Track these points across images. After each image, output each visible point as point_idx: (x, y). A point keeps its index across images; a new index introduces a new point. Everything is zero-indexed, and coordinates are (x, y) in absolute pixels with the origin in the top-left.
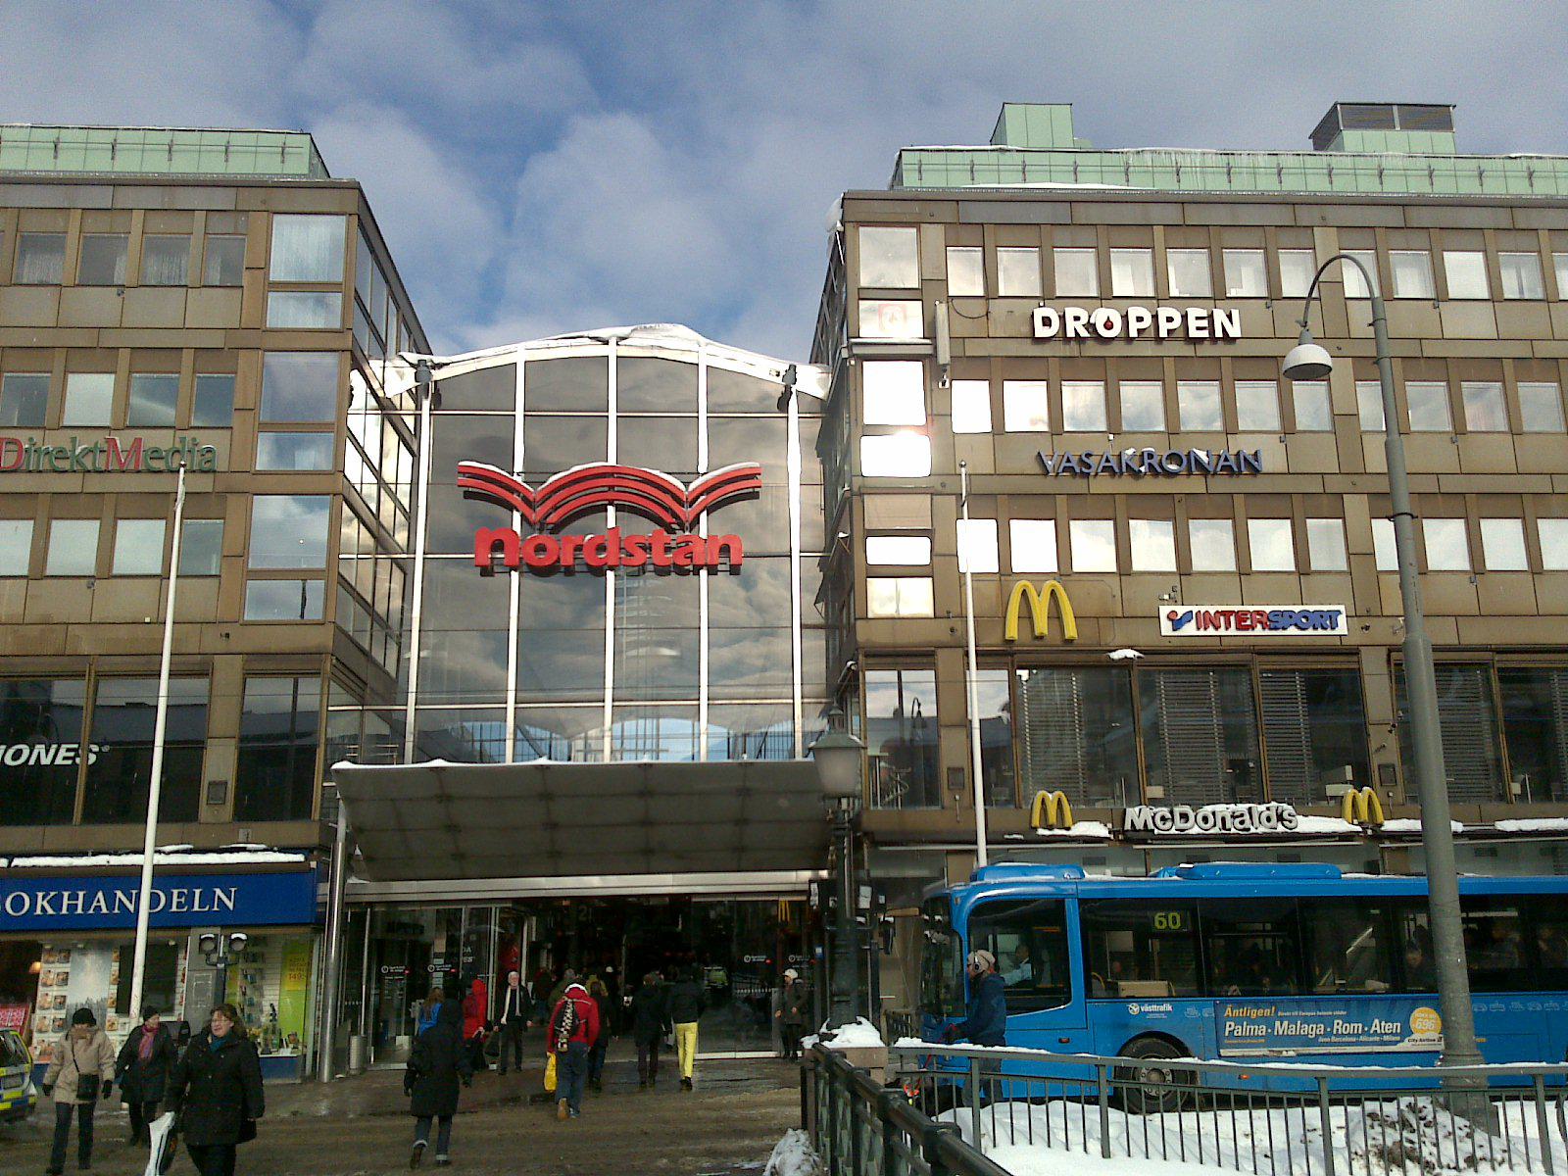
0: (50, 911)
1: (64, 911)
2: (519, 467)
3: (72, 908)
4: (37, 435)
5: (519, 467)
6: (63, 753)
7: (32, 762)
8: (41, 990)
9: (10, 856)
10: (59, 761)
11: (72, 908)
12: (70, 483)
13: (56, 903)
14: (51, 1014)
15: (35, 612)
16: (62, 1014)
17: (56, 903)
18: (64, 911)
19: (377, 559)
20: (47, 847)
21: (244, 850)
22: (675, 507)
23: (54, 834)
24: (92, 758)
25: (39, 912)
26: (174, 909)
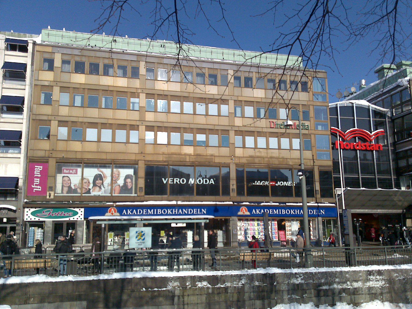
0: (294, 213)
1: (296, 213)
2: (340, 129)
3: (297, 213)
4: (276, 120)
5: (340, 129)
6: (289, 184)
7: (284, 185)
8: (286, 228)
9: (285, 203)
10: (289, 185)
11: (297, 213)
12: (283, 131)
13: (294, 212)
14: (289, 232)
15: (281, 156)
16: (291, 232)
17: (294, 212)
18: (296, 213)
19: (372, 151)
20: (290, 201)
21: (324, 203)
22: (369, 137)
23: (291, 199)
24: (294, 185)
25: (292, 213)
26: (314, 214)
